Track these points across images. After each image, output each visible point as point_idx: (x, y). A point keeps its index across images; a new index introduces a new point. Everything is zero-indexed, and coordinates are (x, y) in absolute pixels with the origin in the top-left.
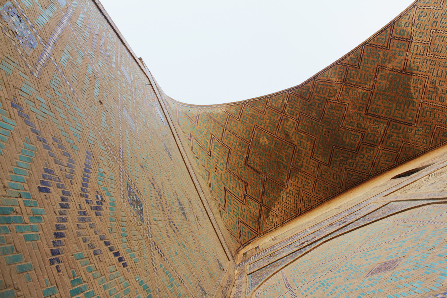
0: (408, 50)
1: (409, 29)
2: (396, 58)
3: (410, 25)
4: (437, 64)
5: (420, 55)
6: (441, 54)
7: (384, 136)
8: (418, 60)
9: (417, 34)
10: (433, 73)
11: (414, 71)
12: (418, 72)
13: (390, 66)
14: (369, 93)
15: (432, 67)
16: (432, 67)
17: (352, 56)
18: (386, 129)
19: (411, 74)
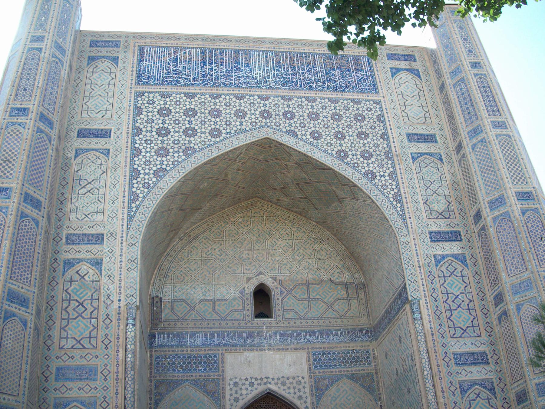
7: (297, 199)
13: (334, 189)
14: (309, 181)
17: (318, 163)
18: (301, 198)
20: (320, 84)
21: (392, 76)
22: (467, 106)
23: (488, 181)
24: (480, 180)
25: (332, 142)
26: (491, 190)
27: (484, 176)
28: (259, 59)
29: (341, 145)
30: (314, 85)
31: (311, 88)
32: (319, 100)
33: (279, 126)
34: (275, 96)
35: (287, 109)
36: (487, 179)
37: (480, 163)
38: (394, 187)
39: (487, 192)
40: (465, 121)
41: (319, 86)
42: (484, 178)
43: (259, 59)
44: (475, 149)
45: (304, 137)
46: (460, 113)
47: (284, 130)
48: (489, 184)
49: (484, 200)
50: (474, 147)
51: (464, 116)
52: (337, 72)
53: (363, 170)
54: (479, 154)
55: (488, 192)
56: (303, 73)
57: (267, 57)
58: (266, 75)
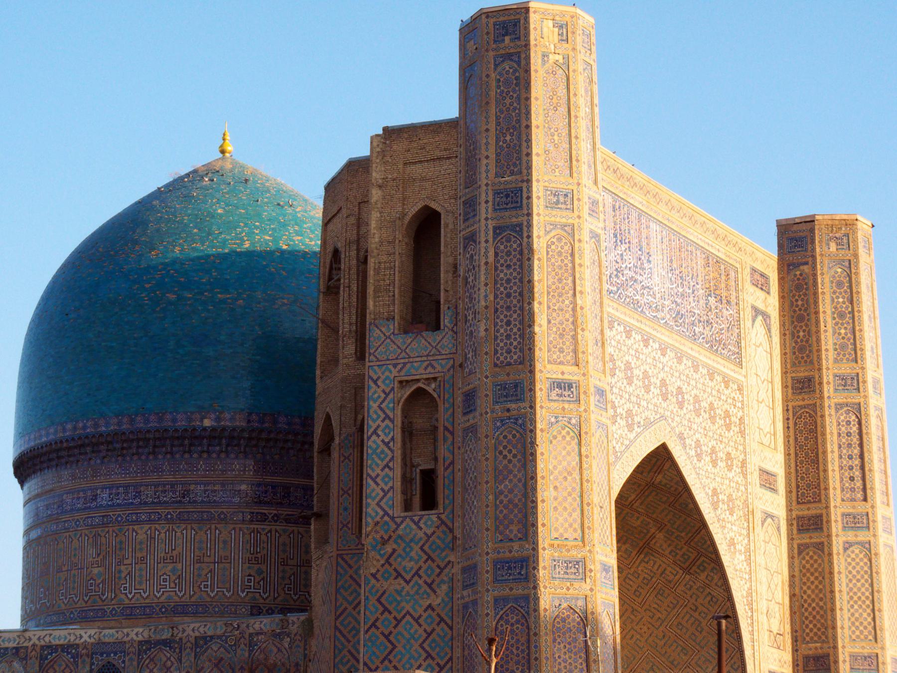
0: (675, 563)
1: (703, 576)
2: (670, 545)
3: (707, 582)
4: (642, 585)
5: (663, 573)
6: (653, 595)
8: (656, 567)
9: (691, 583)
10: (633, 575)
11: (642, 556)
12: (639, 561)
15: (641, 578)
16: (641, 578)
17: (691, 506)
19: (640, 552)
22: (850, 463)
23: (857, 619)
24: (846, 611)
26: (858, 637)
27: (852, 606)
36: (857, 615)
37: (850, 581)
39: (850, 637)
40: (843, 490)
42: (852, 611)
44: (849, 552)
46: (837, 468)
48: (857, 624)
49: (844, 647)
50: (848, 546)
51: (842, 480)
52: (712, 300)
54: (853, 564)
55: (854, 637)
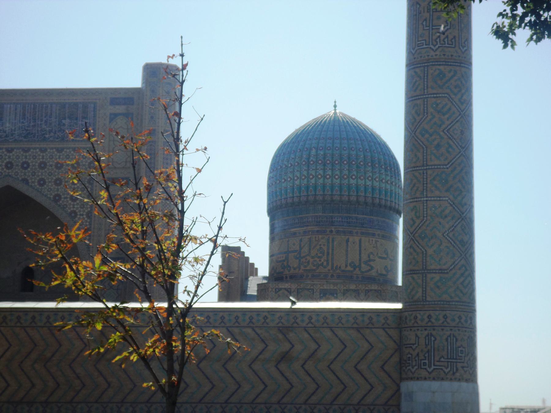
20: (52, 134)
21: (110, 122)
25: (52, 188)
28: (10, 113)
29: (58, 190)
30: (47, 136)
31: (45, 140)
32: (49, 150)
33: (17, 175)
34: (18, 149)
35: (24, 160)
38: (88, 224)
41: (51, 137)
43: (10, 113)
45: (33, 185)
47: (20, 179)
52: (67, 122)
53: (69, 211)
56: (41, 124)
57: (16, 109)
58: (13, 128)
